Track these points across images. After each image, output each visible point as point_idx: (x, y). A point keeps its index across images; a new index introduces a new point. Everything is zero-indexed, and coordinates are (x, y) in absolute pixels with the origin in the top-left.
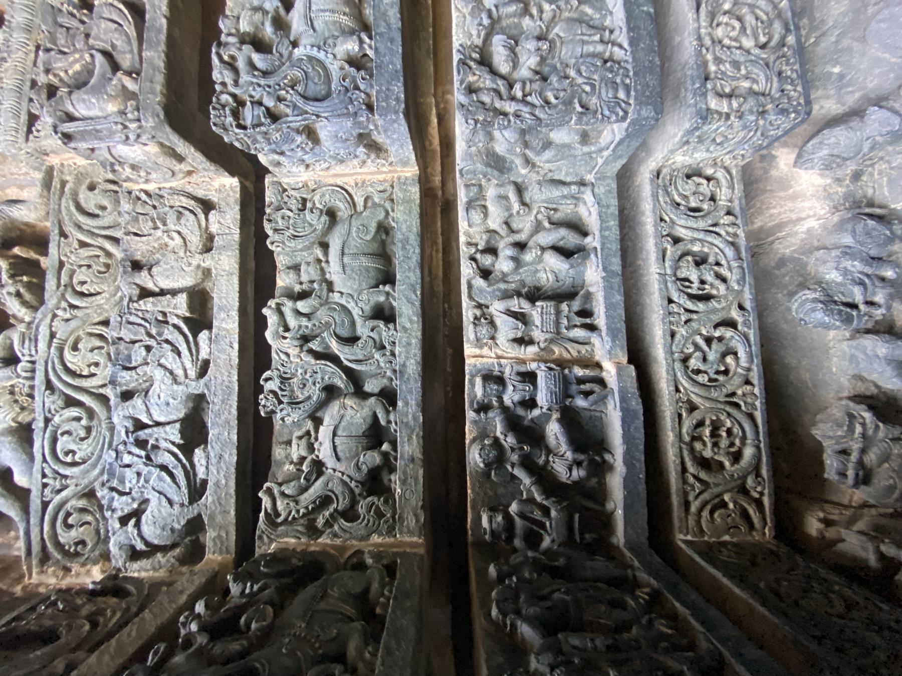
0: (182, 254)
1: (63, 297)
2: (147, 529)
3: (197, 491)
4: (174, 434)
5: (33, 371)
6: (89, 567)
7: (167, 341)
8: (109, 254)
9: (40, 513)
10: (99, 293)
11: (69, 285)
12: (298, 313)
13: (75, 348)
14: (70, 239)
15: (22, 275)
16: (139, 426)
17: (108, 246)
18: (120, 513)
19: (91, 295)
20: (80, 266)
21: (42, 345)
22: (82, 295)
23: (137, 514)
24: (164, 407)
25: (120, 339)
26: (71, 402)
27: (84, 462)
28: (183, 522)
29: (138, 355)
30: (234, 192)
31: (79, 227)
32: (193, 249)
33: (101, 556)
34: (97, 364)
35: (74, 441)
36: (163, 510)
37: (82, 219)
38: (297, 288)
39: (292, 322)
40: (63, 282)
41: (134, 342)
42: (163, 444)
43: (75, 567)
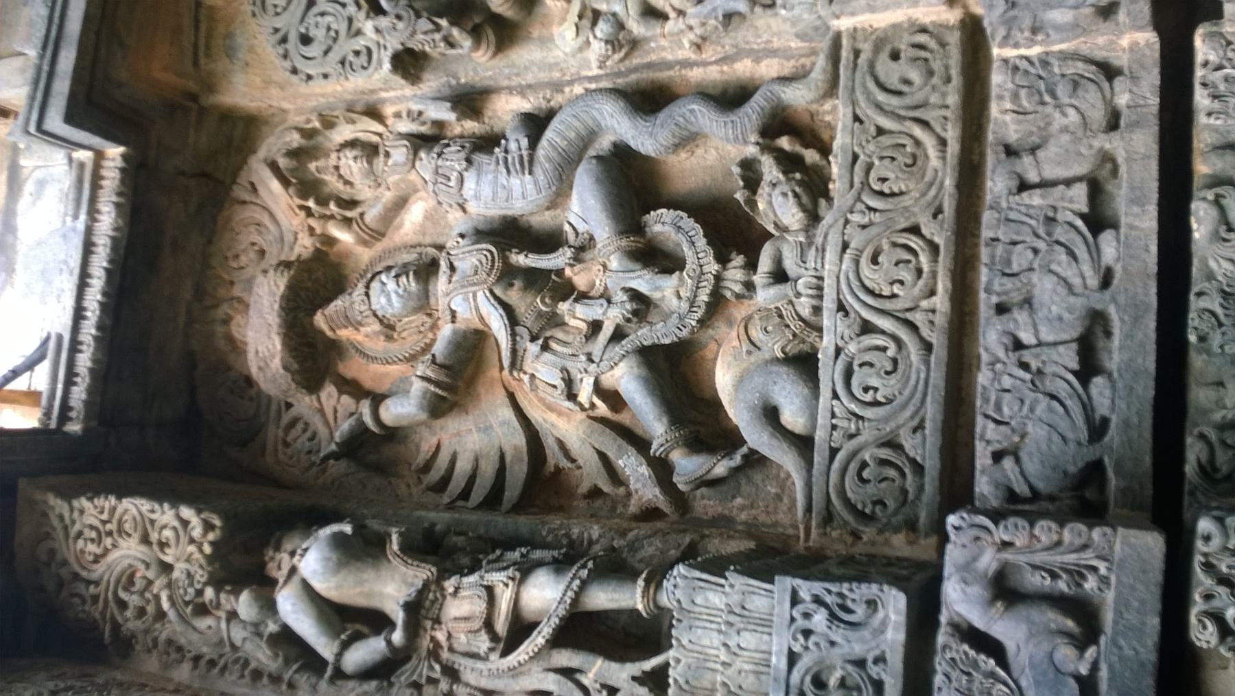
0: (1080, 134)
1: (859, 199)
2: (1031, 466)
3: (1097, 429)
4: (1069, 357)
5: (820, 288)
6: (887, 534)
7: (1058, 243)
8: (917, 143)
9: (827, 462)
10: (901, 193)
11: (865, 183)
13: (874, 260)
14: (867, 124)
15: (793, 172)
16: (1018, 345)
17: (918, 131)
18: (997, 447)
19: (893, 195)
20: (882, 158)
21: (831, 255)
22: (881, 194)
23: (1014, 453)
24: (1057, 324)
25: (997, 240)
26: (867, 328)
27: (889, 401)
28: (1080, 464)
29: (1020, 259)
30: (1152, 50)
31: (879, 107)
32: (1094, 127)
34: (901, 282)
35: (878, 374)
36: (1054, 447)
37: (881, 97)
40: (857, 180)
41: (1014, 243)
42: (1049, 369)
43: (868, 533)
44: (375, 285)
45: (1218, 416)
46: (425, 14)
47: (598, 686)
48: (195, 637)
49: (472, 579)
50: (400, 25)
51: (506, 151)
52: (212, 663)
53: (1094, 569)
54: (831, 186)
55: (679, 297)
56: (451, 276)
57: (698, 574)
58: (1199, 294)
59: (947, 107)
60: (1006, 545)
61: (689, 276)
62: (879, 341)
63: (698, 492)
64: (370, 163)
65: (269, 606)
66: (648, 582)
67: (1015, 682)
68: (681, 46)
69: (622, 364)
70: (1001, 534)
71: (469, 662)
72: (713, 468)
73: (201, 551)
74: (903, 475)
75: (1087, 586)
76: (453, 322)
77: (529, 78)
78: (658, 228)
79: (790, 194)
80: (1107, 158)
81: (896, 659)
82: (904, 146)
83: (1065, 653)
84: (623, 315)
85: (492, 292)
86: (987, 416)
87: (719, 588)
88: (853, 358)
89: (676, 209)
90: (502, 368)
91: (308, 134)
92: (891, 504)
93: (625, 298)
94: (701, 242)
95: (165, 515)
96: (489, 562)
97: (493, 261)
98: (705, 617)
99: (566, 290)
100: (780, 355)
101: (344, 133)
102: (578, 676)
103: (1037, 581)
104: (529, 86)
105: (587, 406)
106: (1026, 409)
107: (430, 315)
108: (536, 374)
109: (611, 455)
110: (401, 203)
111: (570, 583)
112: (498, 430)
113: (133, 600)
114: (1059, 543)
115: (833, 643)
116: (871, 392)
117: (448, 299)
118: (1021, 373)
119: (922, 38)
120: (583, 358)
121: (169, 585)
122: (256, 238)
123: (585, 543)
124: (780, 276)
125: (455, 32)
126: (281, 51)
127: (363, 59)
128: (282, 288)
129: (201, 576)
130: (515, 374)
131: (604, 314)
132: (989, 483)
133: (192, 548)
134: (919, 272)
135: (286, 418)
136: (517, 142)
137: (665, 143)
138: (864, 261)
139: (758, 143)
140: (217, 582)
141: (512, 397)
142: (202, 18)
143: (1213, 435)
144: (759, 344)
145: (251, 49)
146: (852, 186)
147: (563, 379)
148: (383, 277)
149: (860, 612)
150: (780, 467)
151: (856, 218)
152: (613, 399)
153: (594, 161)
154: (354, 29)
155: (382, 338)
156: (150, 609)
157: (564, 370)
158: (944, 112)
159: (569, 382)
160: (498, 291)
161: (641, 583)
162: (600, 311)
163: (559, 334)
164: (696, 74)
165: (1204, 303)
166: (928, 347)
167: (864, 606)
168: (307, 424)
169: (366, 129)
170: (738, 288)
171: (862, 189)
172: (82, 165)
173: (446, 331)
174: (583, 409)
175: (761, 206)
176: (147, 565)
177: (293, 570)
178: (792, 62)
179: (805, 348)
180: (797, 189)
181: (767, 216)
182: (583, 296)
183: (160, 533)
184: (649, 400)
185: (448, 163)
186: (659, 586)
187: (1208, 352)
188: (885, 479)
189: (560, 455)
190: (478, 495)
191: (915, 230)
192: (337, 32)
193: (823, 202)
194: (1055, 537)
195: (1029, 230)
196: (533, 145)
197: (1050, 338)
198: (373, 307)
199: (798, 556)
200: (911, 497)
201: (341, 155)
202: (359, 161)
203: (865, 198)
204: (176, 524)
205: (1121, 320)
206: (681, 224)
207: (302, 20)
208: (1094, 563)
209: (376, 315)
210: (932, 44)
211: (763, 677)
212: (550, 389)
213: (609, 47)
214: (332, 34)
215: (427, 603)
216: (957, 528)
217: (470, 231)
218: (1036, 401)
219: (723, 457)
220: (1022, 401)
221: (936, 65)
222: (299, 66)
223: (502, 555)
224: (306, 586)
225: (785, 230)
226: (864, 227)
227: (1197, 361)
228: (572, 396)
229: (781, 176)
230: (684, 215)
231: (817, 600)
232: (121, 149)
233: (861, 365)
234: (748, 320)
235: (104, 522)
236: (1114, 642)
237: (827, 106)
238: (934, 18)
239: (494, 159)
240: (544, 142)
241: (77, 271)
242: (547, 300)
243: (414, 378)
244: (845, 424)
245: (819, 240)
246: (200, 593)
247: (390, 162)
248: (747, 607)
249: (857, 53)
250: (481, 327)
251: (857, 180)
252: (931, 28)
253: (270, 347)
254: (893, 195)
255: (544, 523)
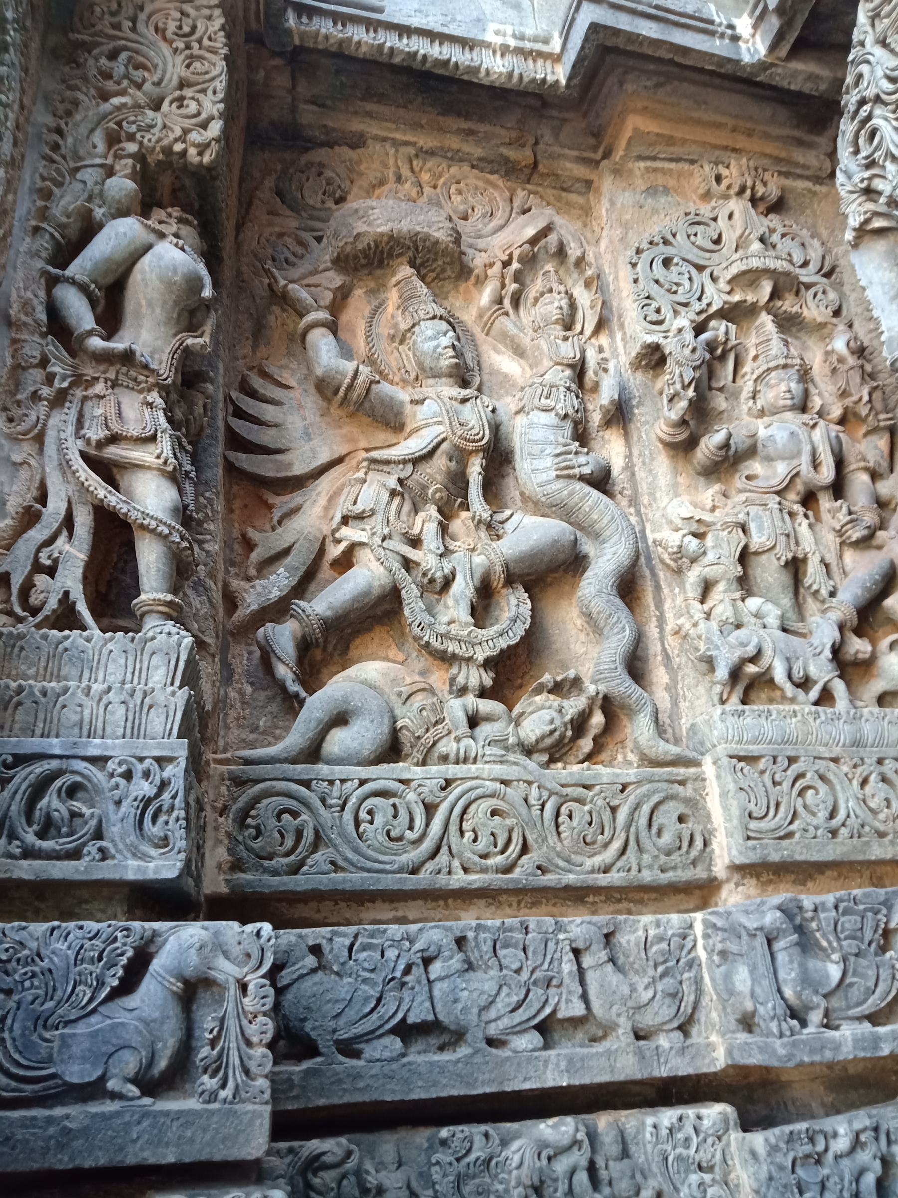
0: (630, 1004)
2: (307, 986)
5: (465, 761)
6: (227, 841)
7: (528, 991)
8: (606, 845)
10: (559, 834)
12: (572, 1172)
13: (494, 813)
15: (572, 729)
16: (427, 962)
17: (617, 845)
18: (326, 948)
19: (557, 826)
20: (590, 813)
22: (558, 815)
24: (451, 998)
26: (430, 809)
30: (709, 1065)
31: (637, 807)
32: (637, 1017)
33: (240, 860)
34: (475, 840)
35: (386, 823)
36: (330, 1005)
37: (646, 809)
38: (600, 1162)
39: (561, 1166)
40: (569, 790)
41: (524, 950)
42: (406, 994)
43: (227, 823)
44: (444, 326)
45: (368, 1166)
46: (697, 375)
47: (56, 555)
48: (83, 130)
49: (162, 420)
50: (687, 352)
51: (576, 453)
52: (56, 147)
53: (224, 1086)
54: (560, 765)
55: (449, 624)
56: (456, 399)
57: (183, 657)
58: (487, 1135)
59: (639, 871)
60: (244, 988)
61: (471, 632)
62: (419, 822)
63: (255, 648)
64: (557, 322)
65: (122, 212)
66: (170, 604)
67: (94, 1011)
68: (679, 616)
69: (382, 569)
70: (255, 981)
71: (72, 417)
72: (284, 663)
73: (176, 140)
74: (288, 854)
75: (205, 1078)
76: (412, 402)
77: (640, 474)
78: (513, 601)
79: (553, 726)
80: (607, 1030)
81: (106, 871)
82: (602, 833)
83: (130, 1063)
84: (430, 569)
85: (444, 440)
86: (356, 937)
87: (169, 680)
88: (400, 797)
89: (532, 617)
90: (367, 450)
91: (580, 262)
92: (257, 844)
93: (446, 571)
94: (503, 643)
95: (212, 105)
96: (178, 439)
97: (474, 441)
98: (138, 667)
99: (446, 514)
100: (399, 724)
101: (583, 297)
102: (65, 533)
103: (207, 1023)
104: (633, 474)
105: (337, 535)
106: (367, 975)
107: (417, 379)
108: (365, 485)
109: (289, 560)
110: (519, 352)
111: (165, 524)
112: (307, 447)
113: (119, 68)
114: (249, 1043)
115: (118, 803)
116: (369, 817)
117: (434, 397)
118: (401, 967)
119: (699, 843)
120: (386, 531)
121: (137, 106)
122: (479, 212)
123: (200, 537)
124: (474, 721)
125: (684, 404)
126: (656, 239)
127: (653, 317)
128: (436, 234)
129: (149, 139)
130: (365, 464)
131: (430, 550)
132: (289, 944)
133: (178, 132)
134: (485, 856)
135: (307, 236)
136: (586, 464)
137: (592, 604)
138: (493, 802)
139: (598, 693)
140: (140, 157)
141: (339, 461)
142: (681, 165)
143: (350, 1164)
144: (408, 703)
145: (655, 211)
146: (562, 786)
147: (364, 511)
148: (451, 334)
149: (156, 830)
150: (287, 729)
151: (534, 792)
152: (345, 562)
153: (572, 537)
154: (679, 308)
155: (392, 332)
156: (110, 85)
157: (373, 512)
158: (635, 867)
159: (360, 517)
160: (444, 446)
161: (169, 597)
162: (431, 547)
163: (407, 507)
164: (652, 631)
165: (479, 1141)
166: (414, 871)
167: (162, 834)
168: (302, 257)
169: (588, 319)
170: (461, 680)
171: (562, 796)
172: (546, 42)
173: (403, 395)
174: (334, 531)
175: (538, 698)
176: (158, 84)
177: (162, 236)
178: (667, 721)
179: (406, 749)
180: (557, 734)
181: (529, 704)
182: (443, 529)
183: (193, 98)
184: (348, 597)
185: (562, 397)
186: (169, 617)
187: (431, 1150)
188: (283, 836)
189: (285, 509)
190: (241, 427)
191: (525, 849)
192: (676, 292)
193: (545, 758)
194: (255, 1040)
195: (539, 963)
196: (582, 478)
197: (436, 993)
198: (422, 323)
199: (200, 754)
200: (266, 863)
201: (563, 295)
202: (558, 311)
203: (553, 799)
204: (203, 116)
205: (458, 1061)
206: (519, 622)
207: (684, 259)
208: (231, 1084)
209: (413, 326)
210: (694, 853)
211: (76, 731)
212: (352, 498)
213: (675, 549)
214: (674, 288)
215: (133, 373)
216: (258, 934)
217: (499, 419)
218: (373, 984)
219: (295, 673)
220: (373, 971)
221: (675, 857)
222: (643, 255)
223: (187, 452)
224: (148, 247)
225: (518, 724)
226: (526, 800)
227: (421, 1136)
228: (345, 520)
229: (568, 718)
230: (527, 626)
231: (163, 785)
232: (563, 82)
233: (394, 806)
234: (431, 691)
235: (199, 42)
236: (145, 1115)
237: (631, 757)
238: (717, 852)
239: (569, 441)
240: (588, 489)
241: (446, 31)
242: (438, 495)
243: (356, 363)
244: (336, 793)
245: (512, 757)
246: (131, 137)
247: (559, 342)
248: (152, 710)
249: (682, 783)
250: (408, 429)
251: (566, 791)
252: (708, 850)
253: (379, 221)
254: (557, 826)
255: (217, 494)
